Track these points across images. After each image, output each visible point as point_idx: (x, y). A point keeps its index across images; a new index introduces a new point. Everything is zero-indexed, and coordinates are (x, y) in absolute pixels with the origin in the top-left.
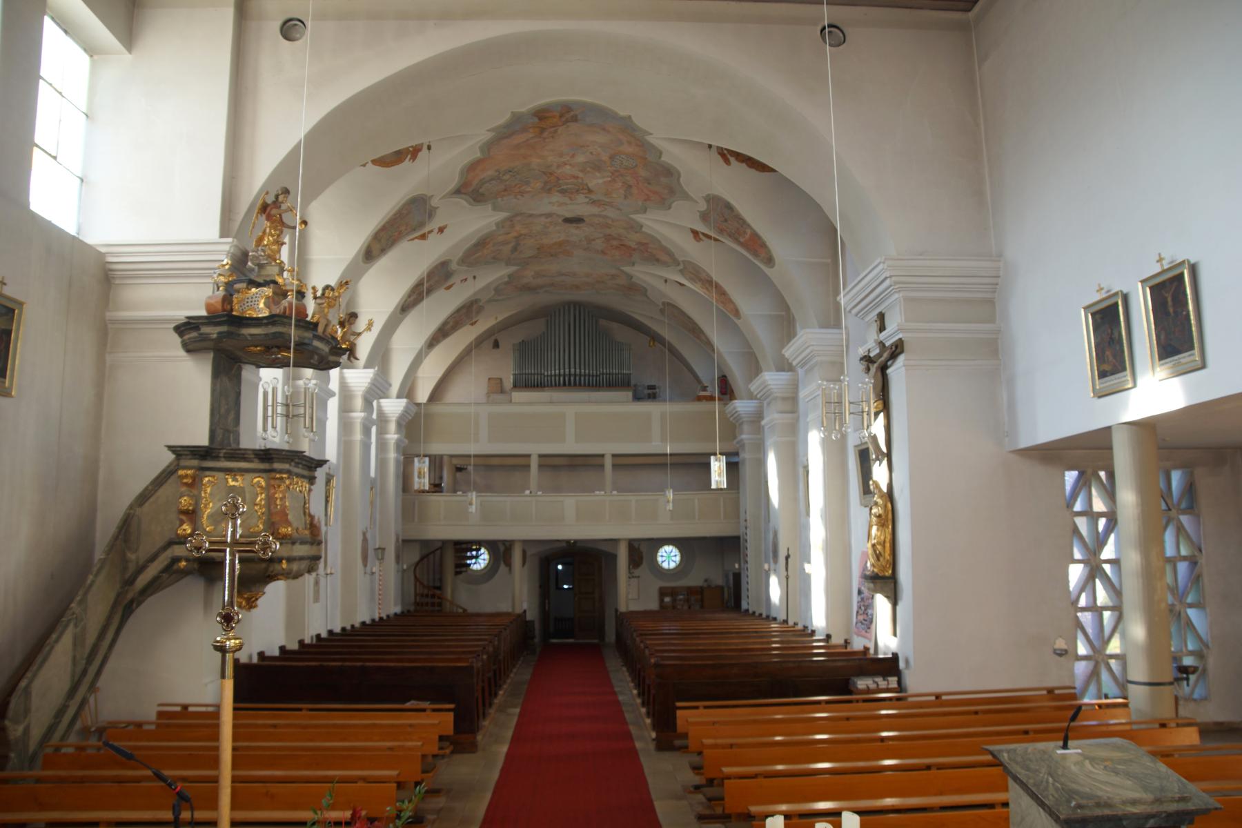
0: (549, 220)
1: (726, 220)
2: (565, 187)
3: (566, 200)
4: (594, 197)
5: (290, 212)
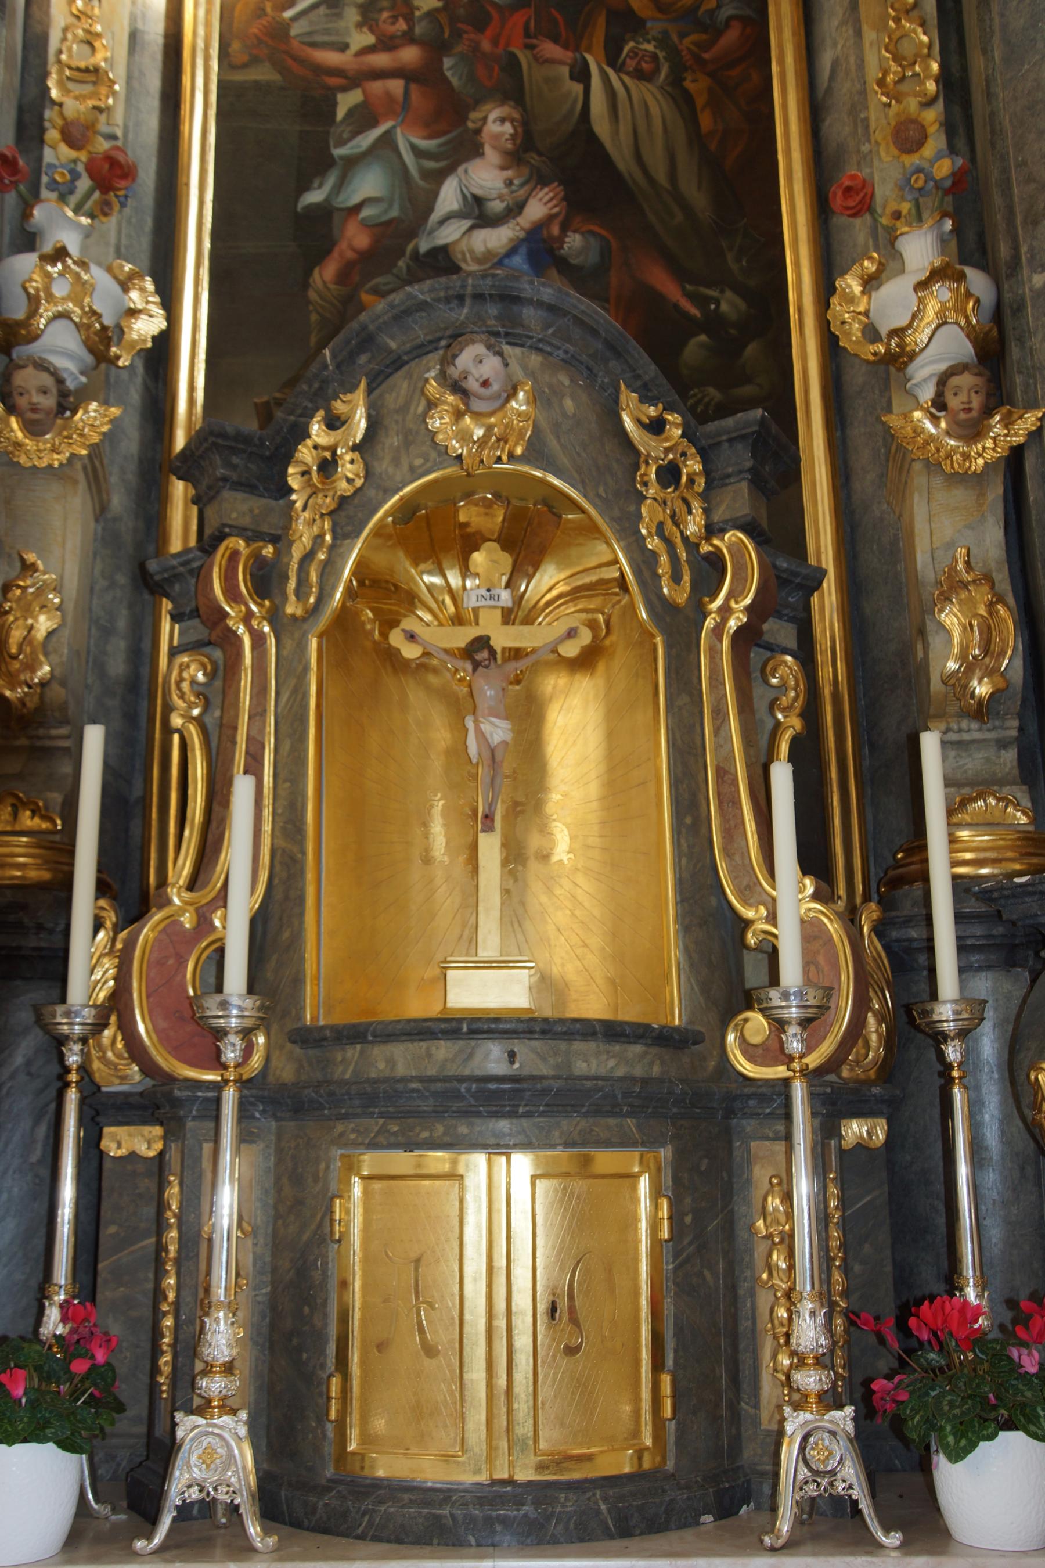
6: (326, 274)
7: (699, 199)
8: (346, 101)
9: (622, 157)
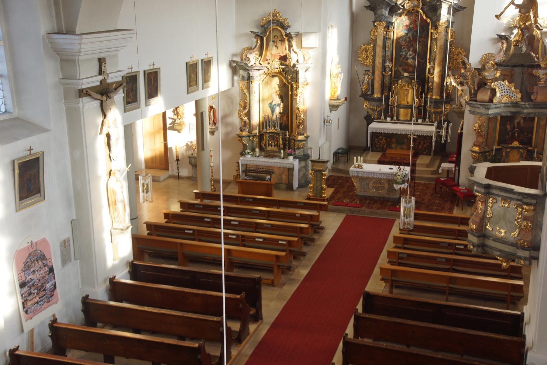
6: (401, 59)
7: (423, 55)
8: (403, 47)
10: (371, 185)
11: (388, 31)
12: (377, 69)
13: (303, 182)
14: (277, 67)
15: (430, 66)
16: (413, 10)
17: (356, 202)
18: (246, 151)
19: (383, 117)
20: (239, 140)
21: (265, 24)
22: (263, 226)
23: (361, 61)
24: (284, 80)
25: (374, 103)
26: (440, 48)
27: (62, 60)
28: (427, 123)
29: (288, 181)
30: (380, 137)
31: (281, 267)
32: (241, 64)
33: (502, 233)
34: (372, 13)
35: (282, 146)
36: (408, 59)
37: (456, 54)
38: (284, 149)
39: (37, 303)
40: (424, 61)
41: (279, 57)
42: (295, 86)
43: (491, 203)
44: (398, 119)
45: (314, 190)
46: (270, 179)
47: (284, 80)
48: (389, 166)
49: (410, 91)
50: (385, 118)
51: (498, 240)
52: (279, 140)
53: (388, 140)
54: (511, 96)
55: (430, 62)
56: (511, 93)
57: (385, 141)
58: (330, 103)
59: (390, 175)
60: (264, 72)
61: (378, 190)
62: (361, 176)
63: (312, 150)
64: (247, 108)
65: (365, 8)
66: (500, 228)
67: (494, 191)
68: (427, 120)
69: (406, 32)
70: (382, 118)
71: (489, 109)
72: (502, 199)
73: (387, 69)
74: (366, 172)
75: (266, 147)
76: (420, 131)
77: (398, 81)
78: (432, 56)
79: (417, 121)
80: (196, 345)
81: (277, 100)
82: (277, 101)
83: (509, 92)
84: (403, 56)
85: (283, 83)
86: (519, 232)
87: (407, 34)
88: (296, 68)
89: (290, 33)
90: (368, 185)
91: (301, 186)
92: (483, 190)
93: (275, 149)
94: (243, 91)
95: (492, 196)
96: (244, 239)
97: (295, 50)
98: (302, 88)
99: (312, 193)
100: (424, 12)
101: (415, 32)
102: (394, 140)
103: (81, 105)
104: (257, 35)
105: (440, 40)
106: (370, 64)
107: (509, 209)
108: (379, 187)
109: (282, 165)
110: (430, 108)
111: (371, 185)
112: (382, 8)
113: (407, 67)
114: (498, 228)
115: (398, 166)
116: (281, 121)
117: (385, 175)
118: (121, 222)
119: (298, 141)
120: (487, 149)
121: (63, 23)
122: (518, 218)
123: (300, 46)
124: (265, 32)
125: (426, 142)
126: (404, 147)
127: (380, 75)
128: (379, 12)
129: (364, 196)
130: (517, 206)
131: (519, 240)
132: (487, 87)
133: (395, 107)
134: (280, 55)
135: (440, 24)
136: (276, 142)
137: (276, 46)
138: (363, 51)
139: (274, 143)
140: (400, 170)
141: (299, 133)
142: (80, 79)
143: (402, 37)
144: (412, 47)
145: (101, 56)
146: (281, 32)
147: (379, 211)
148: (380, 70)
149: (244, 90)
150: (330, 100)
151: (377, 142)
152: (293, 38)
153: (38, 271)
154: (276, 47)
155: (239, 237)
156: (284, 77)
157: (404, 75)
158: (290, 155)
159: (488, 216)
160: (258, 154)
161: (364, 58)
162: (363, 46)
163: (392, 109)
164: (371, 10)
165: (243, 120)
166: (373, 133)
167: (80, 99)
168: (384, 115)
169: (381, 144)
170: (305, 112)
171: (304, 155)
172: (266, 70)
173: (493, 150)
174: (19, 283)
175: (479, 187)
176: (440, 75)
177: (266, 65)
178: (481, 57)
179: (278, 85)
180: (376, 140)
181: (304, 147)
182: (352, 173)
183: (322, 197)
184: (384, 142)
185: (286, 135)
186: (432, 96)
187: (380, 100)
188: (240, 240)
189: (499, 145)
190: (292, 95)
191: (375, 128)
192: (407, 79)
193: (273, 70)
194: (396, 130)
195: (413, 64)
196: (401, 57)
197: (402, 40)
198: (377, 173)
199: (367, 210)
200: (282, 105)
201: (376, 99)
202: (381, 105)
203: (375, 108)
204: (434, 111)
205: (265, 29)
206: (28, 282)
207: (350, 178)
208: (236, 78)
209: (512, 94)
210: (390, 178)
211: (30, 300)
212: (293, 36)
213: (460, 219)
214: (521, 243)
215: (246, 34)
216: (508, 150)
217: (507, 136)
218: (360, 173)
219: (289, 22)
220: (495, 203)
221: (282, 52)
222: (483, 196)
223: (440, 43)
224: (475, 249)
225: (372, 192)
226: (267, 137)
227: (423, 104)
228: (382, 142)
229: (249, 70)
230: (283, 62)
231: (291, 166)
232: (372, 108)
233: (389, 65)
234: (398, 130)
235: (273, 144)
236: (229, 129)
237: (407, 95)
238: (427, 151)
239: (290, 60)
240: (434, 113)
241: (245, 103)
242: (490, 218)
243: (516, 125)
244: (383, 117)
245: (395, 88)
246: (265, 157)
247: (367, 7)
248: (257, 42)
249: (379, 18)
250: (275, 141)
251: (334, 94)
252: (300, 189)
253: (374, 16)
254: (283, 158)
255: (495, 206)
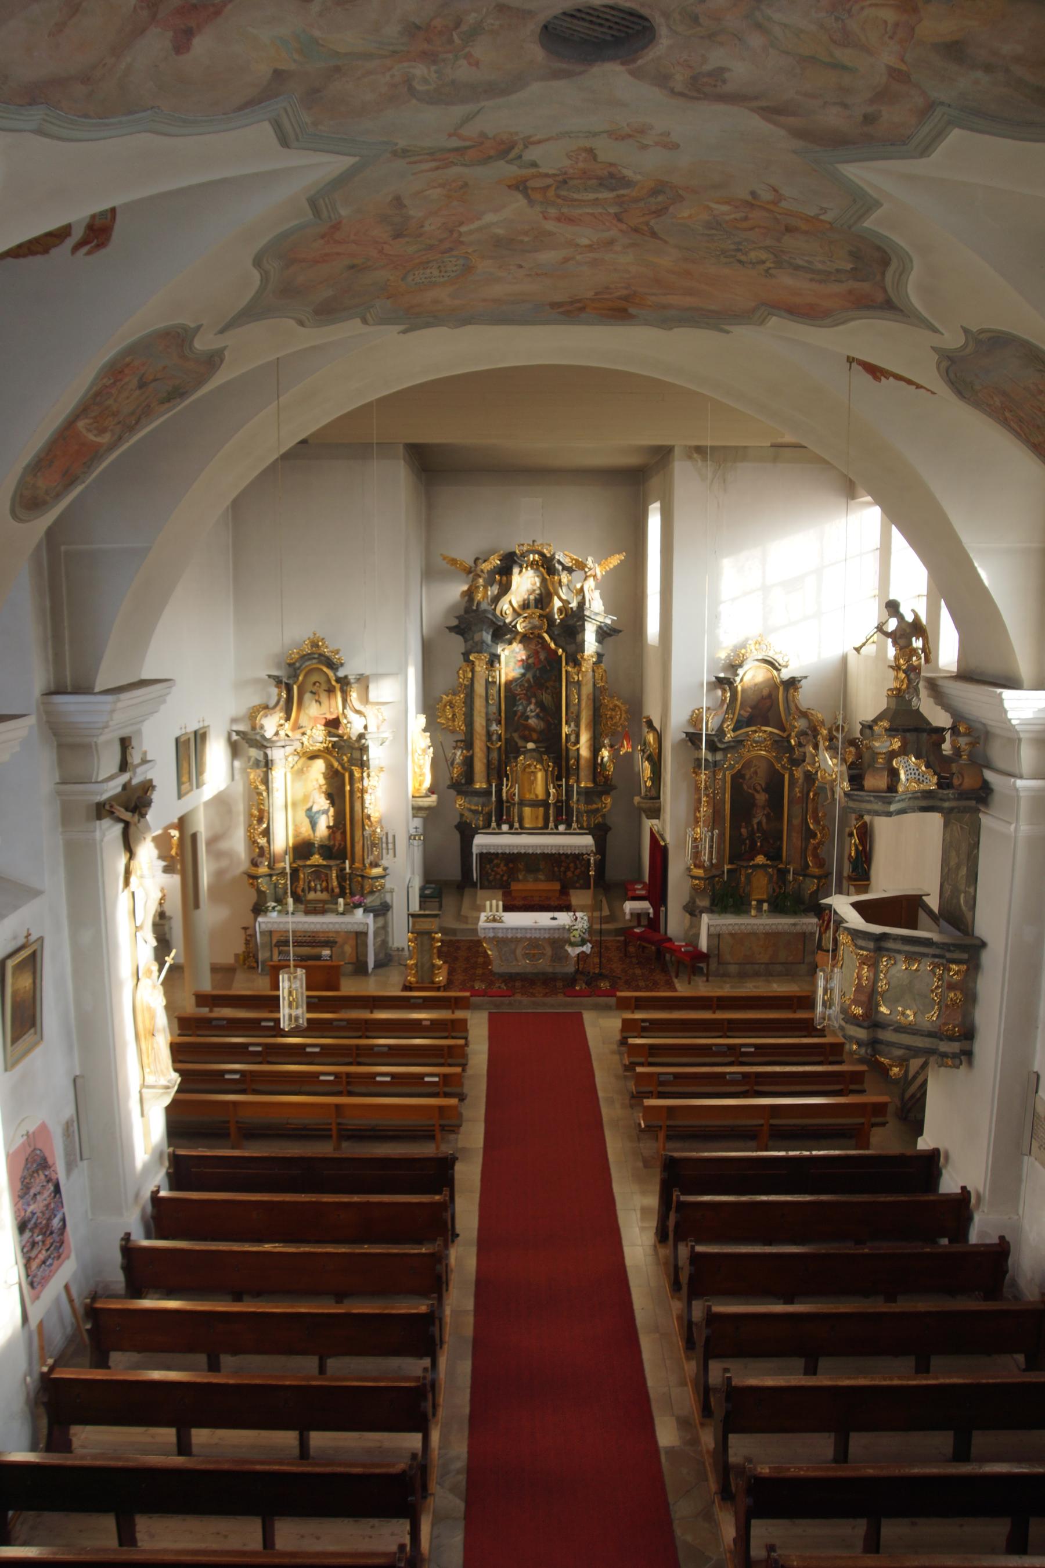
0: (717, 57)
1: (142, 385)
2: (605, 195)
3: (609, 152)
4: (509, 170)
5: (857, 645)
6: (516, 718)
8: (518, 697)
9: (546, 704)
10: (519, 952)
11: (491, 670)
12: (478, 737)
13: (382, 956)
14: (321, 739)
15: (570, 729)
16: (532, 633)
17: (499, 987)
18: (269, 904)
19: (494, 824)
20: (252, 884)
21: (296, 661)
22: (372, 1049)
23: (443, 724)
24: (336, 764)
25: (476, 799)
26: (588, 697)
27: (60, 746)
28: (494, 831)
29: (357, 958)
30: (495, 861)
31: (446, 1128)
32: (253, 737)
33: (908, 1016)
34: (460, 638)
35: (337, 890)
36: (528, 718)
37: (610, 709)
38: (342, 894)
39: (44, 1262)
40: (556, 722)
41: (323, 721)
42: (357, 774)
43: (885, 966)
44: (522, 827)
45: (417, 971)
46: (331, 957)
47: (336, 764)
48: (551, 914)
49: (540, 775)
50: (499, 826)
51: (901, 1029)
52: (332, 879)
53: (511, 865)
54: (921, 780)
55: (566, 723)
56: (921, 775)
57: (505, 868)
58: (414, 803)
59: (557, 931)
60: (295, 750)
61: (533, 961)
62: (503, 937)
63: (394, 894)
64: (265, 820)
65: (447, 630)
66: (905, 1009)
67: (890, 945)
68: (574, 825)
69: (522, 671)
70: (492, 827)
71: (890, 803)
72: (905, 958)
73: (495, 737)
74: (512, 929)
75: (305, 895)
76: (567, 846)
77: (516, 758)
78: (572, 713)
79: (557, 828)
80: (423, 1309)
81: (321, 803)
82: (322, 804)
83: (917, 774)
84: (519, 714)
85: (334, 770)
86: (940, 1009)
87: (523, 675)
88: (363, 741)
89: (346, 677)
90: (514, 952)
91: (378, 965)
92: (871, 945)
93: (324, 896)
94: (258, 789)
95: (887, 953)
96: (350, 1080)
97: (357, 708)
98: (376, 778)
99: (414, 977)
100: (551, 638)
101: (538, 672)
102: (521, 866)
103: (98, 834)
104: (278, 681)
105: (586, 684)
106: (460, 729)
107: (919, 973)
108: (534, 955)
109: (343, 926)
110: (576, 803)
111: (519, 952)
112: (482, 630)
113: (527, 733)
114: (900, 1009)
115: (572, 913)
116: (332, 843)
117: (547, 931)
118: (162, 1071)
119: (372, 878)
120: (715, 872)
121: (68, 673)
122: (937, 987)
123: (365, 699)
124: (296, 676)
125: (579, 866)
126: (540, 876)
127: (485, 749)
128: (477, 637)
129: (507, 973)
130: (934, 967)
131: (945, 1024)
132: (878, 766)
133: (514, 804)
134: (326, 718)
135: (585, 657)
136: (324, 884)
137: (319, 702)
138: (445, 706)
139: (321, 885)
140: (576, 919)
141: (374, 864)
142: (97, 782)
143: (515, 680)
144: (535, 696)
145: (124, 732)
146: (327, 676)
147: (549, 1000)
148: (484, 738)
149: (260, 787)
150: (413, 797)
151: (490, 871)
152: (353, 686)
153: (39, 1193)
154: (318, 703)
155: (341, 1078)
156: (334, 757)
157: (526, 747)
158: (357, 906)
159: (880, 990)
160: (291, 908)
161: (449, 719)
162: (444, 696)
163: (508, 808)
164: (457, 633)
165: (258, 843)
166: (481, 855)
167: (98, 822)
168: (496, 821)
169: (497, 874)
170: (380, 821)
171: (381, 903)
172: (297, 745)
173: (723, 872)
174: (18, 1224)
175: (865, 940)
176: (591, 745)
177: (298, 736)
178: (690, 714)
179: (324, 774)
180: (488, 866)
181: (383, 888)
182: (485, 933)
183: (433, 982)
184: (502, 870)
185: (345, 869)
186: (578, 781)
187: (487, 793)
188: (344, 1083)
189: (731, 862)
190: (352, 792)
191: (486, 846)
192: (534, 754)
193: (312, 746)
194: (525, 846)
195: (539, 727)
196: (516, 715)
197: (517, 685)
198: (531, 929)
199: (525, 1000)
200: (332, 811)
201: (480, 792)
202: (490, 801)
203: (480, 808)
204: (586, 809)
205: (295, 670)
206: (30, 1220)
207: (479, 943)
208: (237, 764)
209: (923, 776)
210: (556, 936)
211: (34, 1259)
212: (352, 681)
213: (715, 999)
214: (948, 1030)
215: (257, 681)
216: (750, 871)
217: (743, 847)
218: (500, 931)
219: (343, 656)
220: (892, 965)
221: (330, 712)
222: (872, 954)
223: (587, 690)
224: (863, 1051)
225: (523, 965)
226: (306, 875)
227: (564, 798)
228: (499, 870)
229: (266, 747)
230: (333, 730)
231: (361, 928)
232: (473, 808)
233: (496, 730)
234: (529, 846)
235: (318, 887)
236: (224, 863)
237: (533, 782)
238: (581, 882)
239: (349, 725)
240: (586, 812)
241: (261, 811)
242: (884, 992)
243: (755, 826)
244: (495, 824)
245: (511, 769)
246: (307, 912)
247: (451, 629)
248: (280, 696)
249: (478, 647)
250: (323, 881)
251: (420, 785)
252: (379, 971)
253: (463, 644)
254: (343, 914)
255: (893, 971)
